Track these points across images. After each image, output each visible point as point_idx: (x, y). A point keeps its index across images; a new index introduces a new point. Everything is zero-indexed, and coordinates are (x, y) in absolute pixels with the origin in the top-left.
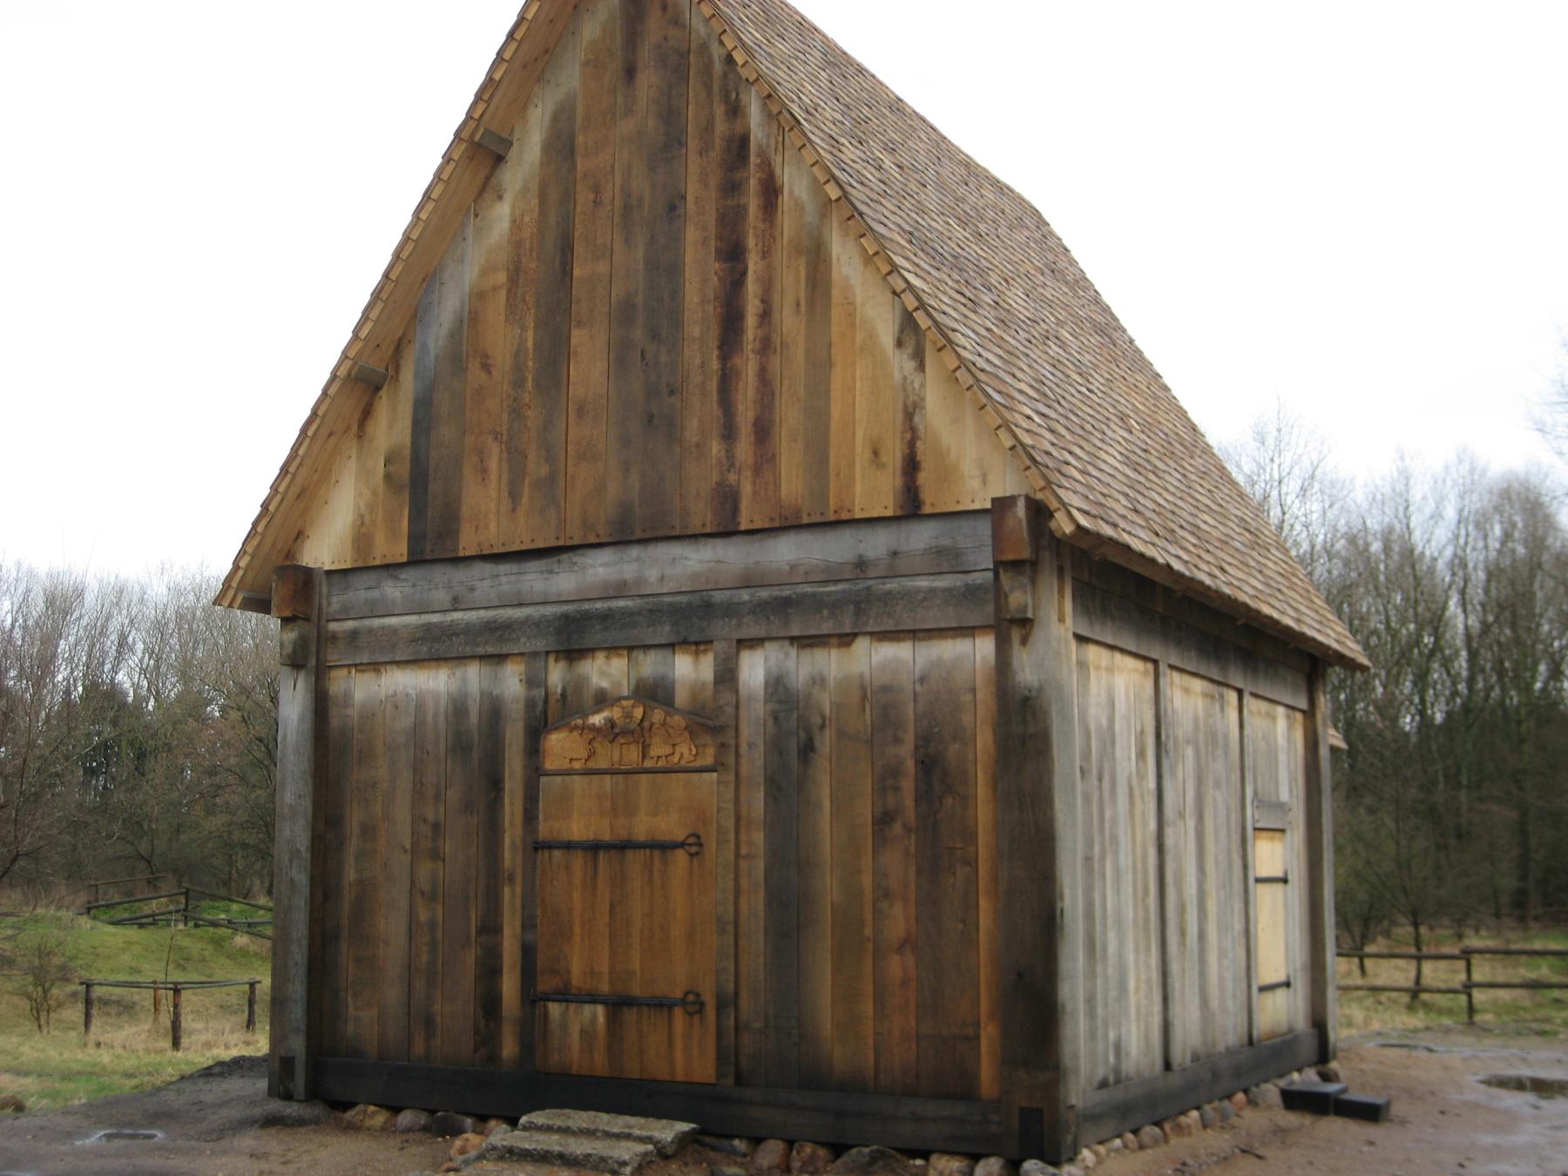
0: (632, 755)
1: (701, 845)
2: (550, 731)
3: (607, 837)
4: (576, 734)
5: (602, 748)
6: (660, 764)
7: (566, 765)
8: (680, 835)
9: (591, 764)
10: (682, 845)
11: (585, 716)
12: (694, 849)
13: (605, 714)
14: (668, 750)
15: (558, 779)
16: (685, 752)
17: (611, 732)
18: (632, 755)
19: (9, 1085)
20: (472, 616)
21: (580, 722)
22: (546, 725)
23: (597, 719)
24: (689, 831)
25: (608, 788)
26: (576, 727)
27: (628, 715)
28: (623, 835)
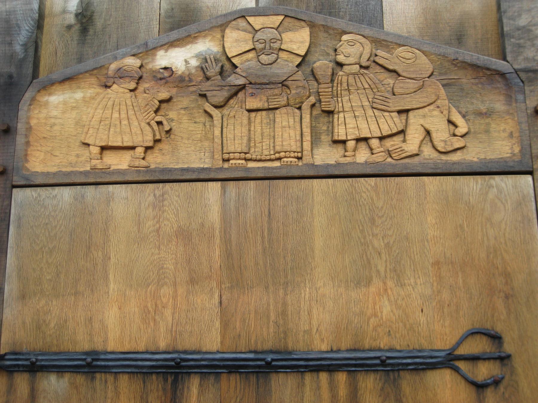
0: (286, 133)
1: (504, 359)
2: (48, 86)
3: (211, 341)
4: (119, 91)
5: (183, 119)
6: (362, 156)
7: (84, 162)
8: (440, 333)
9: (157, 160)
10: (449, 360)
11: (148, 50)
12: (484, 371)
13: (205, 46)
14: (389, 123)
15: (66, 194)
16: (431, 128)
17: (223, 86)
18: (286, 133)
19: (368, 402)
20: (471, 53)
21: (132, 62)
22: (35, 74)
23: (179, 59)
24: (465, 326)
25: (214, 215)
26: (121, 75)
27: (270, 48)
28: (259, 335)
